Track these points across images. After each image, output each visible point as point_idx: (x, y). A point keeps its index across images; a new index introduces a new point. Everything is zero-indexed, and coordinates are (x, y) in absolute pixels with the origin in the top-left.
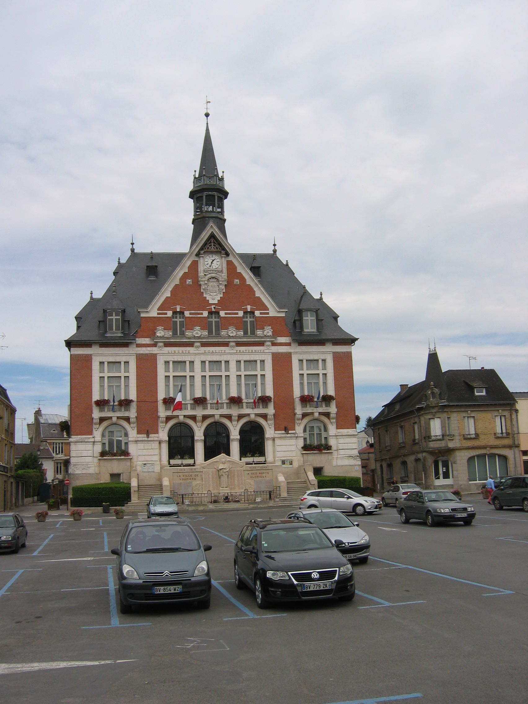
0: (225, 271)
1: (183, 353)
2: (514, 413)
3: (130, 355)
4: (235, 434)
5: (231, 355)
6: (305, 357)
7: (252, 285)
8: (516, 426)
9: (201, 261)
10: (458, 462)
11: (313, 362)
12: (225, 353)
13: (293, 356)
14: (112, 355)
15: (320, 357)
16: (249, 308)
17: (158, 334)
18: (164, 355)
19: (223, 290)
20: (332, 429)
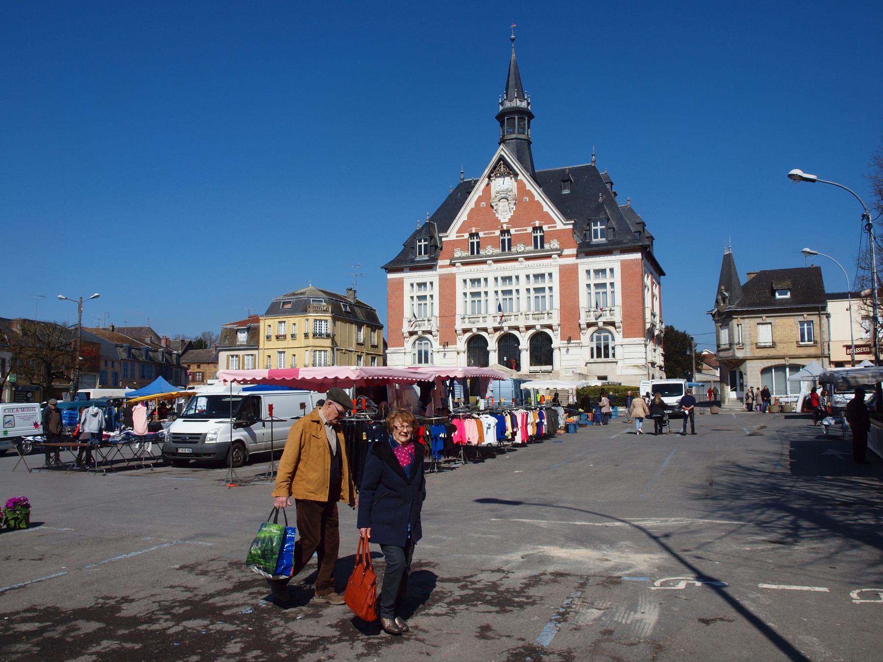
0: (515, 191)
2: (824, 317)
3: (434, 276)
4: (524, 343)
5: (521, 269)
6: (592, 267)
7: (541, 200)
8: (826, 332)
9: (493, 184)
10: (748, 373)
11: (601, 272)
13: (579, 267)
14: (420, 277)
15: (607, 266)
16: (537, 224)
18: (462, 273)
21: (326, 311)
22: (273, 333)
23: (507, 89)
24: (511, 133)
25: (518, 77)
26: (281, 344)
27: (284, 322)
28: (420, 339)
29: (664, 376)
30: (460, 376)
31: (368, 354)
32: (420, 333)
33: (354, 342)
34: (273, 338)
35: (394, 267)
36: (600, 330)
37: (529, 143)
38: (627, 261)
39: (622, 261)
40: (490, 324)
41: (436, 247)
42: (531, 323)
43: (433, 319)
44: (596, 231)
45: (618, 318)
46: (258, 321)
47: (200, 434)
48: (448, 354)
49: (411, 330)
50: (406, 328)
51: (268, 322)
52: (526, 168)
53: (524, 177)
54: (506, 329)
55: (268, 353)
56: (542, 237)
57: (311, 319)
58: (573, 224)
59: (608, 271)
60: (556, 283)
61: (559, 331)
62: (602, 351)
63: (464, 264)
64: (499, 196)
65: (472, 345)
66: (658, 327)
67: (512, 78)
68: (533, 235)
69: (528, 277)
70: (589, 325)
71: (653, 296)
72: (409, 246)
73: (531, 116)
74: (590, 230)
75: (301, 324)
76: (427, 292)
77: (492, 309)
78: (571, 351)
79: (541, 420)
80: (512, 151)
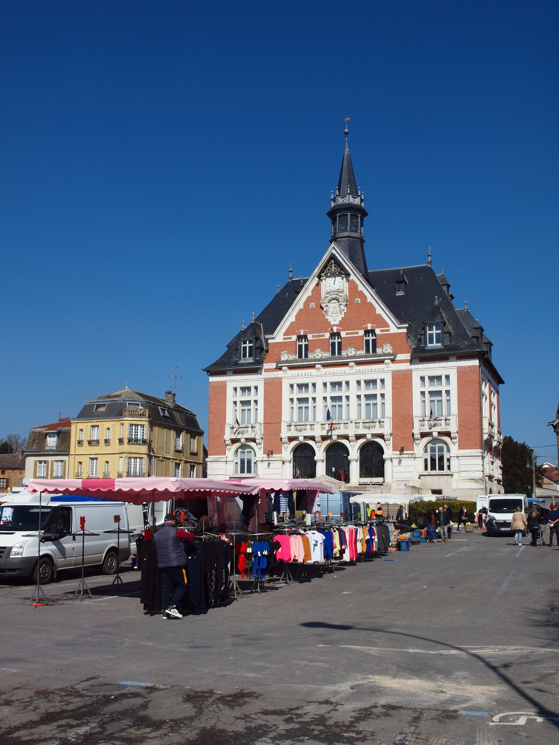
0: (346, 292)
1: (303, 374)
3: (259, 380)
4: (354, 454)
5: (350, 374)
9: (323, 283)
12: (345, 374)
13: (413, 372)
16: (369, 327)
17: (282, 359)
18: (289, 377)
19: (344, 310)
20: (455, 449)
21: (142, 415)
22: (85, 438)
23: (339, 186)
24: (343, 231)
25: (351, 173)
26: (94, 450)
27: (98, 426)
28: (243, 447)
29: (503, 491)
30: (286, 489)
31: (186, 462)
32: (243, 441)
33: (172, 449)
34: (85, 443)
35: (216, 369)
36: (434, 441)
37: (362, 241)
38: (464, 367)
39: (458, 368)
40: (318, 432)
41: (262, 349)
42: (361, 431)
43: (257, 426)
44: (431, 335)
45: (453, 428)
46: (69, 424)
47: (5, 548)
48: (273, 464)
49: (234, 437)
50: (228, 435)
51: (80, 426)
52: (358, 268)
53: (356, 277)
54: (334, 438)
55: (79, 459)
56: (374, 341)
57: (127, 424)
58: (407, 328)
59: (443, 378)
60: (388, 390)
61: (391, 441)
62: (437, 463)
63: (291, 368)
64: (330, 297)
65: (298, 454)
66: (496, 438)
67: (345, 173)
68: (365, 338)
69: (359, 382)
70: (423, 435)
71: (491, 405)
72: (233, 348)
73: (364, 214)
74: (425, 335)
75: (116, 429)
76: (251, 397)
77: (321, 416)
78: (404, 462)
79: (371, 536)
80: (343, 250)
